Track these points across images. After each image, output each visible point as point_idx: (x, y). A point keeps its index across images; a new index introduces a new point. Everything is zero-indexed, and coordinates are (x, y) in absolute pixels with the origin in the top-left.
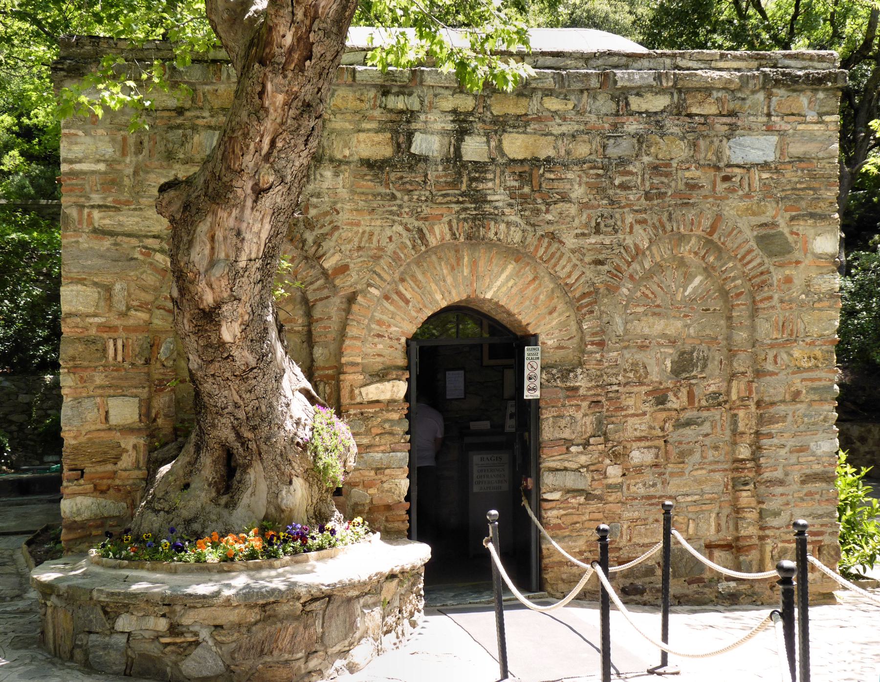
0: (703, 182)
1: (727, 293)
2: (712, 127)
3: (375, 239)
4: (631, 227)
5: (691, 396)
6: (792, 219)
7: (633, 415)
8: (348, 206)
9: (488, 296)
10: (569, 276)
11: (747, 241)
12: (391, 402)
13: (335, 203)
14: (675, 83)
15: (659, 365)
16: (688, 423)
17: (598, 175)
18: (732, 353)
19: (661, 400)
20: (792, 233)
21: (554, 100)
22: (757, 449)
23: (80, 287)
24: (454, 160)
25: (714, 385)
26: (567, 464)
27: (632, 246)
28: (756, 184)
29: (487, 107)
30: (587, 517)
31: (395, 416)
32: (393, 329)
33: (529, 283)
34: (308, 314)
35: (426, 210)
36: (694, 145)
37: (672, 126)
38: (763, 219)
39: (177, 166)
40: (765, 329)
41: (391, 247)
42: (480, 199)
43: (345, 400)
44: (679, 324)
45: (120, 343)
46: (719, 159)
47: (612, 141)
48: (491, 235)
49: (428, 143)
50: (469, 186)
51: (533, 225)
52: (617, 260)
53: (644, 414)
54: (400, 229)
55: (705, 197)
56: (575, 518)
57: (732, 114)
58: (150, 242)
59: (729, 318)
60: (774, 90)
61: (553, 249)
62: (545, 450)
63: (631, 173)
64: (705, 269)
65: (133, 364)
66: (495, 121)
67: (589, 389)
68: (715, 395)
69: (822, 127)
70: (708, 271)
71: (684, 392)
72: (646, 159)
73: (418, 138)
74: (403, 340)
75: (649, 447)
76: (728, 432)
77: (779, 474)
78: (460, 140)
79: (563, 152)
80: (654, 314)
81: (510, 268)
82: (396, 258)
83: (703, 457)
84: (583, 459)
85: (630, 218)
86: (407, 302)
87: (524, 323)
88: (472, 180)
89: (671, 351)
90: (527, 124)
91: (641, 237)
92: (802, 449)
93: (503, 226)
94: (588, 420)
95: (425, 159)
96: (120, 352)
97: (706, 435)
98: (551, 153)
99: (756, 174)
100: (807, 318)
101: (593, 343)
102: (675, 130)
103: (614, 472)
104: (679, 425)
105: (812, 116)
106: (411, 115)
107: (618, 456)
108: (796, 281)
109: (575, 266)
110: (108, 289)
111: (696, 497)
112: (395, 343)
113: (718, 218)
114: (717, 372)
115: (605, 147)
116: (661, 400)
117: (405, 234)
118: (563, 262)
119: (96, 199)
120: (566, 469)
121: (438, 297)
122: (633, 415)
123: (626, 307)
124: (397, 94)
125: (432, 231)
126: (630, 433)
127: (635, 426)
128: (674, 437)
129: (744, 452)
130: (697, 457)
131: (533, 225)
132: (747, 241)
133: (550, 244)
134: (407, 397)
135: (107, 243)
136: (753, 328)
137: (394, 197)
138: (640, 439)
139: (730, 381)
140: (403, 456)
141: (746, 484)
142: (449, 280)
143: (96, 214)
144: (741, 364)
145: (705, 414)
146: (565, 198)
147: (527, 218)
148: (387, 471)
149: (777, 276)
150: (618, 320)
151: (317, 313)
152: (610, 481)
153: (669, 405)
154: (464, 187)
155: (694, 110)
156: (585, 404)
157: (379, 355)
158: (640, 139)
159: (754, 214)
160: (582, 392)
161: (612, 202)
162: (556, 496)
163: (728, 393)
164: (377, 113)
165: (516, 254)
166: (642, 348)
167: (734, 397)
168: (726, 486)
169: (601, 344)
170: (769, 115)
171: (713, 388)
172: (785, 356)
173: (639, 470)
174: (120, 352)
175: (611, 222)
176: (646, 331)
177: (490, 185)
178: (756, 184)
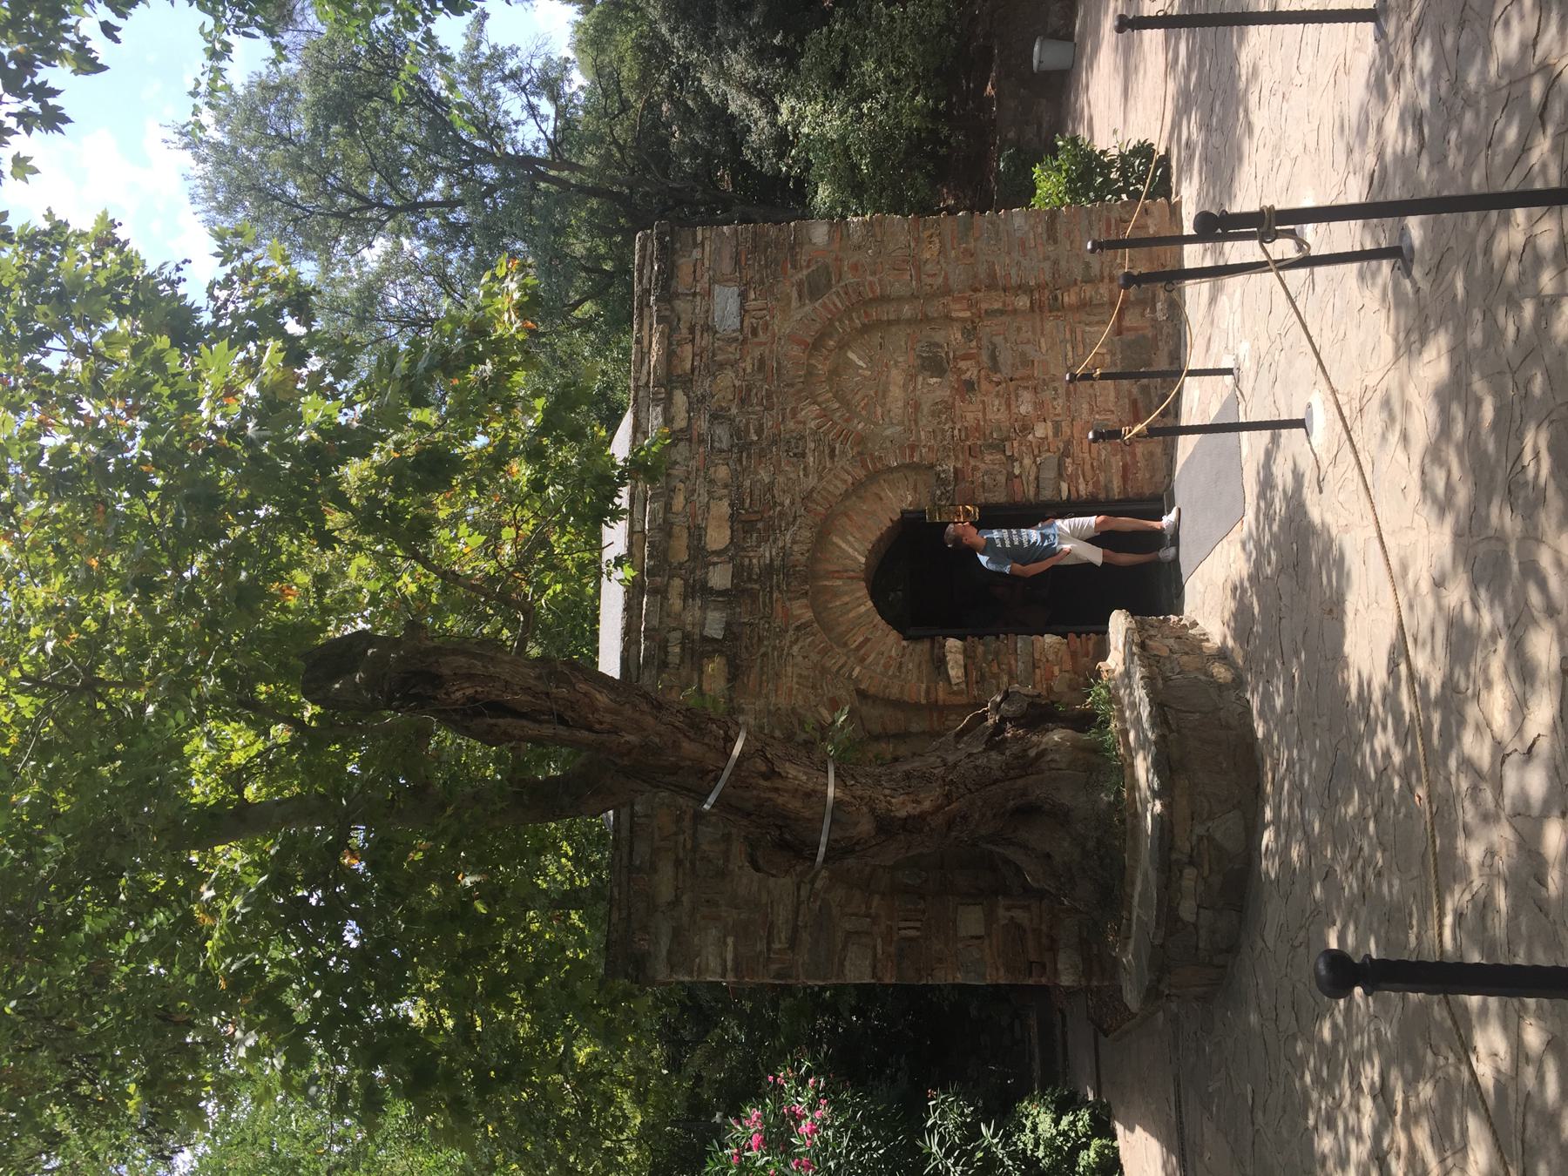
0: (757, 354)
1: (864, 325)
2: (703, 350)
3: (805, 673)
4: (799, 422)
5: (966, 357)
6: (794, 267)
7: (984, 414)
8: (773, 700)
9: (863, 560)
10: (845, 481)
11: (815, 309)
12: (965, 652)
13: (769, 712)
14: (662, 386)
15: (934, 389)
16: (993, 358)
17: (749, 457)
18: (926, 319)
19: (970, 386)
20: (808, 266)
21: (675, 502)
22: (1022, 288)
23: (847, 963)
24: (729, 597)
25: (957, 335)
26: (1032, 478)
28: (760, 303)
29: (681, 565)
31: (980, 649)
32: (893, 653)
33: (851, 520)
34: (877, 738)
35: (778, 623)
36: (722, 366)
37: (703, 386)
38: (795, 295)
39: (731, 867)
40: (899, 285)
41: (814, 657)
42: (769, 570)
43: (963, 700)
44: (894, 372)
45: (903, 924)
46: (736, 340)
47: (716, 445)
48: (803, 559)
49: (714, 624)
50: (756, 581)
51: (795, 518)
53: (983, 402)
54: (795, 649)
55: (771, 352)
56: (1087, 467)
57: (692, 330)
58: (804, 893)
59: (889, 323)
62: (1017, 499)
63: (748, 424)
64: (841, 348)
65: (924, 912)
66: (692, 558)
67: (957, 458)
68: (964, 331)
69: (707, 243)
70: (843, 346)
71: (963, 365)
72: (734, 411)
73: (709, 632)
74: (905, 643)
75: (1017, 396)
76: (1004, 318)
77: (1047, 265)
78: (711, 591)
79: (725, 492)
80: (884, 397)
81: (836, 539)
82: (824, 652)
83: (1028, 342)
84: (1027, 461)
85: (791, 425)
86: (867, 640)
87: (889, 524)
89: (920, 379)
90: (699, 527)
91: (809, 412)
92: (1023, 244)
93: (796, 548)
94: (988, 458)
95: (728, 626)
96: (911, 924)
97: (1006, 339)
98: (726, 502)
99: (751, 305)
100: (891, 247)
101: (912, 456)
102: (707, 384)
103: (1041, 430)
104: (995, 367)
105: (696, 254)
106: (686, 636)
107: (1027, 428)
108: (855, 259)
109: (836, 477)
110: (849, 934)
111: (1069, 347)
112: (908, 651)
113: (792, 338)
114: (943, 333)
115: (721, 451)
116: (970, 386)
117: (800, 644)
118: (831, 488)
119: (761, 946)
120: (1037, 478)
121: (863, 609)
122: (984, 414)
123: (876, 424)
124: (666, 653)
125: (798, 617)
126: (1002, 416)
127: (997, 413)
128: (1006, 371)
129: (1023, 302)
130: (1028, 348)
131: (795, 518)
132: (815, 309)
133: (814, 501)
134: (961, 638)
135: (805, 936)
136: (900, 299)
137: (765, 655)
138: (1009, 406)
139: (952, 319)
140: (1021, 642)
141: (1056, 298)
142: (846, 599)
143: (776, 946)
144: (934, 309)
145: (985, 342)
146: (770, 488)
147: (787, 524)
148: (1037, 656)
149: (849, 278)
150: (888, 432)
151: (876, 728)
152: (1050, 434)
153: (974, 378)
154: (757, 586)
155: (688, 366)
156: (972, 462)
157: (920, 665)
158: (715, 417)
160: (959, 465)
161: (775, 442)
162: (1064, 486)
163: (964, 320)
164: (684, 672)
165: (822, 535)
166: (917, 407)
167: (968, 314)
168: (1057, 317)
169: (913, 448)
170: (694, 295)
171: (959, 336)
172: (928, 266)
173: (1039, 405)
174: (911, 924)
176: (900, 404)
177: (755, 561)
178: (760, 303)
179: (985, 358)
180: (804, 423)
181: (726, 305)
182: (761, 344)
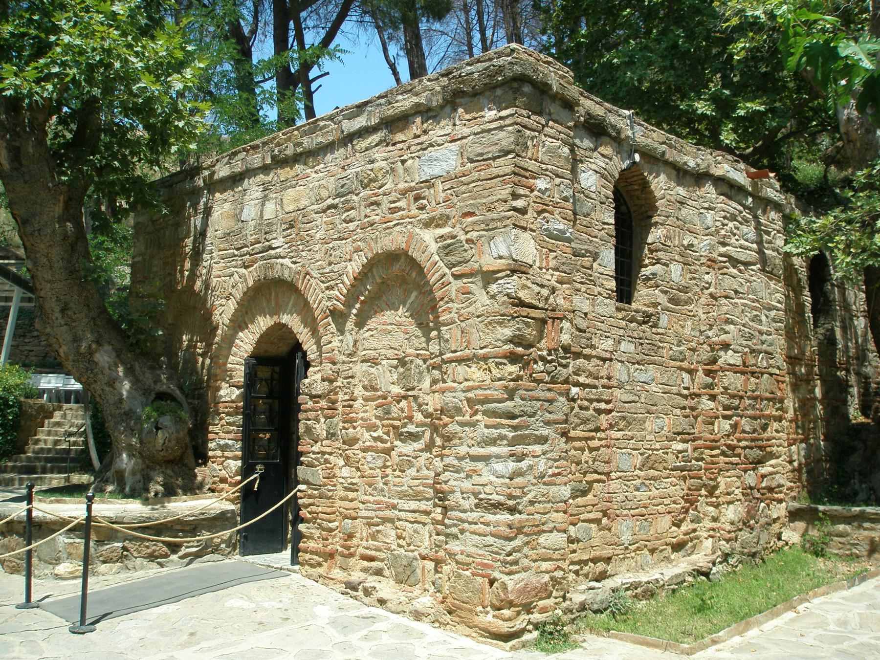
10: (314, 302)
27: (351, 271)
30: (320, 509)
52: (341, 285)
60: (458, 101)
61: (306, 281)
78: (263, 205)
81: (293, 297)
83: (418, 471)
85: (349, 248)
88: (266, 233)
93: (279, 267)
159: (438, 226)
175: (338, 252)
179: (411, 428)
180: (350, 260)
181: (444, 160)
182: (409, 205)
